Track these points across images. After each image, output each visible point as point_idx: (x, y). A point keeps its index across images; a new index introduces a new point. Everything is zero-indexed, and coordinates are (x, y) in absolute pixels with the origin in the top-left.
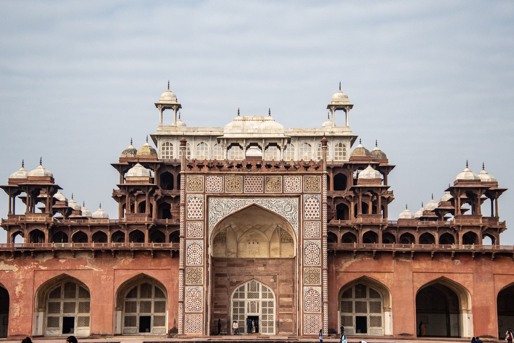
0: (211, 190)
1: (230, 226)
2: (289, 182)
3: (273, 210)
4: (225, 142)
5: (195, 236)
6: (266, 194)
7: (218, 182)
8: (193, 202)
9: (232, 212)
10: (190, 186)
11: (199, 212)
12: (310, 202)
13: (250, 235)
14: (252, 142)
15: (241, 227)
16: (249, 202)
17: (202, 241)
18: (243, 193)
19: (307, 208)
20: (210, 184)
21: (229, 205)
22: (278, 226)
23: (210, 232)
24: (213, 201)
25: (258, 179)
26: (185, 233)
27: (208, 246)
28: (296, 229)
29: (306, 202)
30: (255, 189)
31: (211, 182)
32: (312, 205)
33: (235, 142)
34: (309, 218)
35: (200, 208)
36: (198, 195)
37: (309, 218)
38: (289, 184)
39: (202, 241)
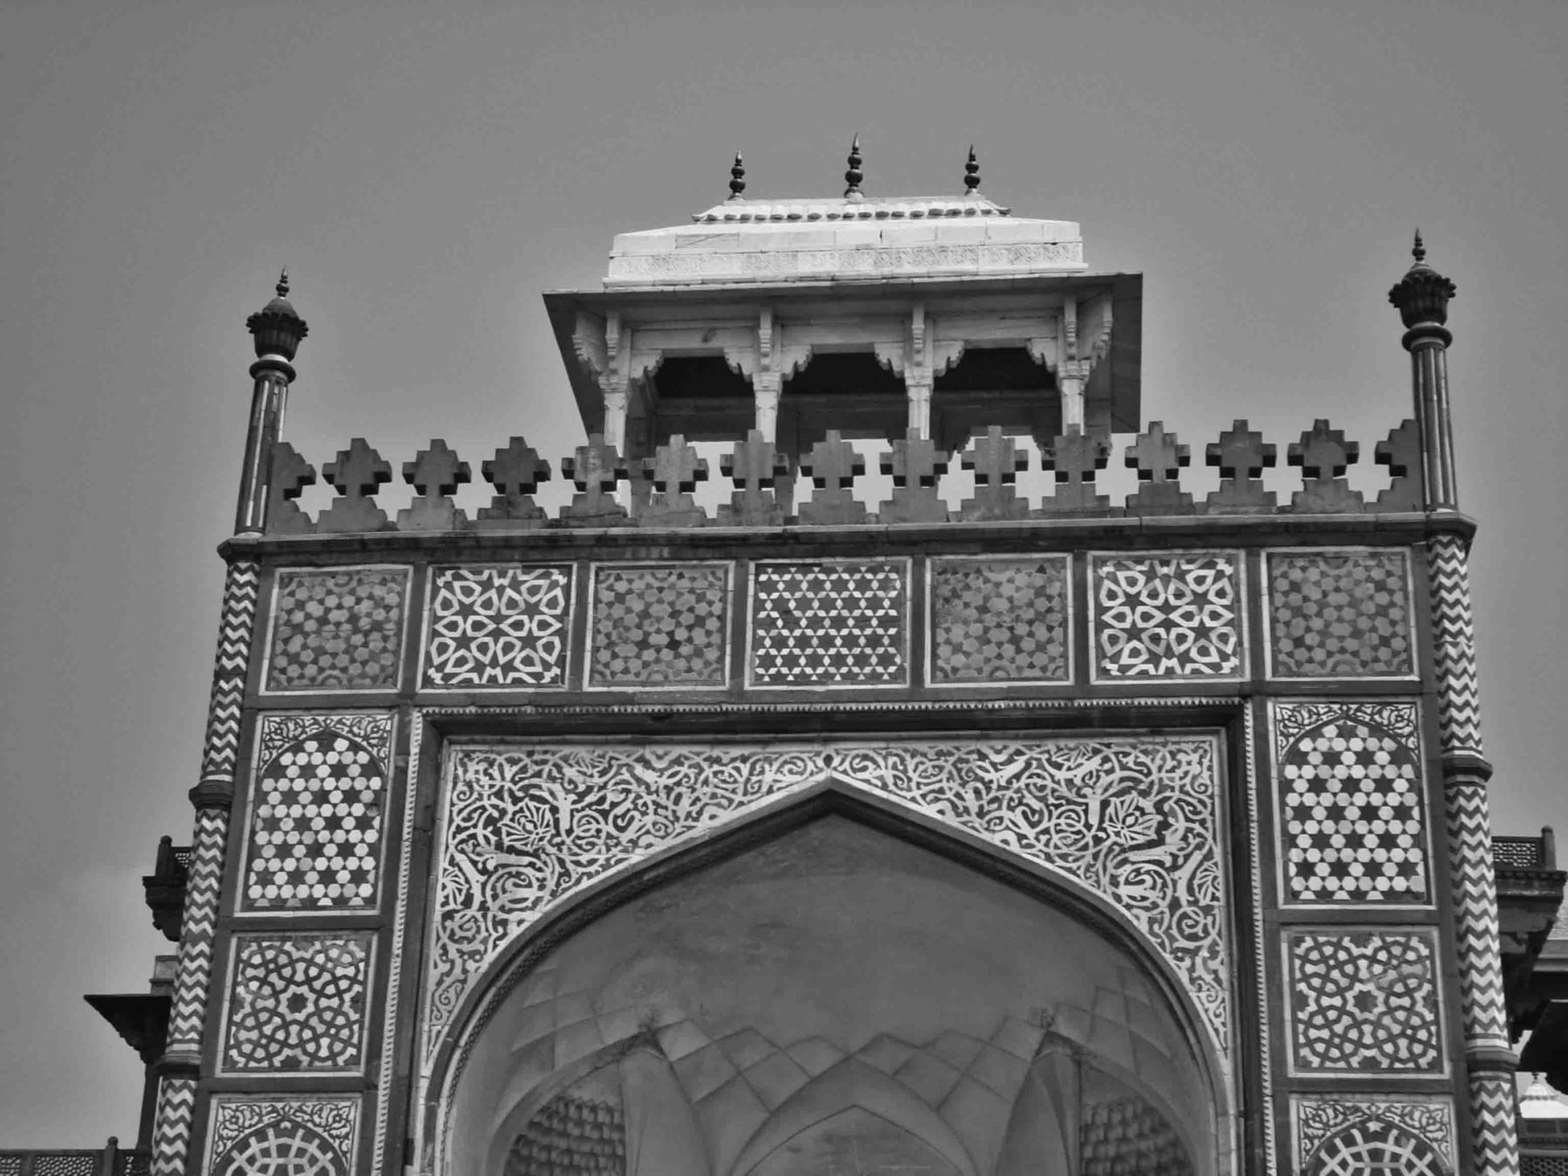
0: (464, 673)
1: (649, 1038)
2: (1133, 601)
3: (996, 839)
4: (612, 335)
5: (291, 1064)
6: (936, 696)
7: (532, 610)
8: (308, 771)
9: (637, 857)
10: (295, 645)
11: (346, 850)
12: (1332, 758)
13: (829, 1138)
14: (834, 339)
15: (748, 1057)
16: (789, 775)
17: (352, 1110)
18: (738, 694)
19: (1303, 813)
20: (466, 626)
21: (611, 797)
22: (1051, 1037)
23: (434, 1029)
24: (475, 778)
25: (863, 585)
26: (207, 1038)
27: (401, 1151)
28: (1212, 1007)
29: (1298, 758)
30: (838, 660)
31: (466, 611)
32: (1351, 785)
33: (689, 343)
34: (1324, 895)
35: (363, 824)
36: (348, 718)
37: (1324, 895)
38: (1133, 618)
39: (352, 1110)
